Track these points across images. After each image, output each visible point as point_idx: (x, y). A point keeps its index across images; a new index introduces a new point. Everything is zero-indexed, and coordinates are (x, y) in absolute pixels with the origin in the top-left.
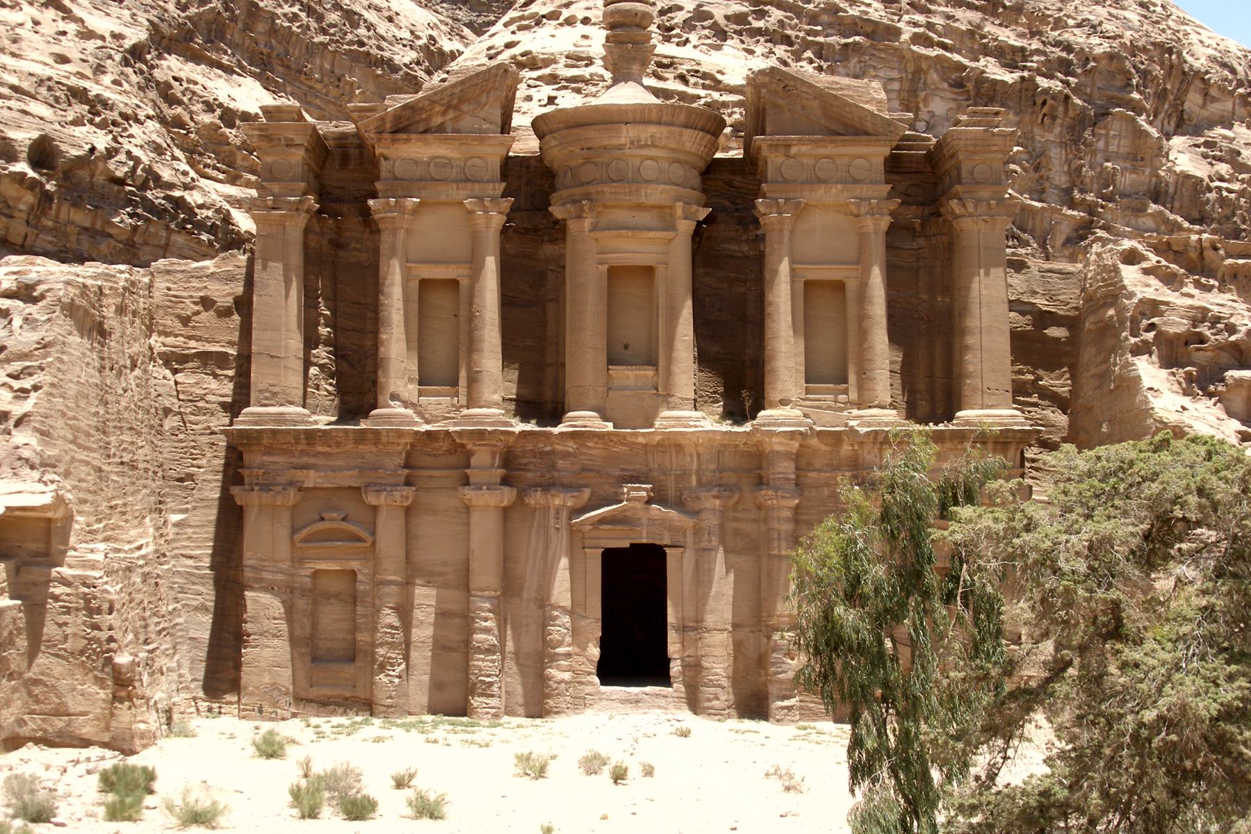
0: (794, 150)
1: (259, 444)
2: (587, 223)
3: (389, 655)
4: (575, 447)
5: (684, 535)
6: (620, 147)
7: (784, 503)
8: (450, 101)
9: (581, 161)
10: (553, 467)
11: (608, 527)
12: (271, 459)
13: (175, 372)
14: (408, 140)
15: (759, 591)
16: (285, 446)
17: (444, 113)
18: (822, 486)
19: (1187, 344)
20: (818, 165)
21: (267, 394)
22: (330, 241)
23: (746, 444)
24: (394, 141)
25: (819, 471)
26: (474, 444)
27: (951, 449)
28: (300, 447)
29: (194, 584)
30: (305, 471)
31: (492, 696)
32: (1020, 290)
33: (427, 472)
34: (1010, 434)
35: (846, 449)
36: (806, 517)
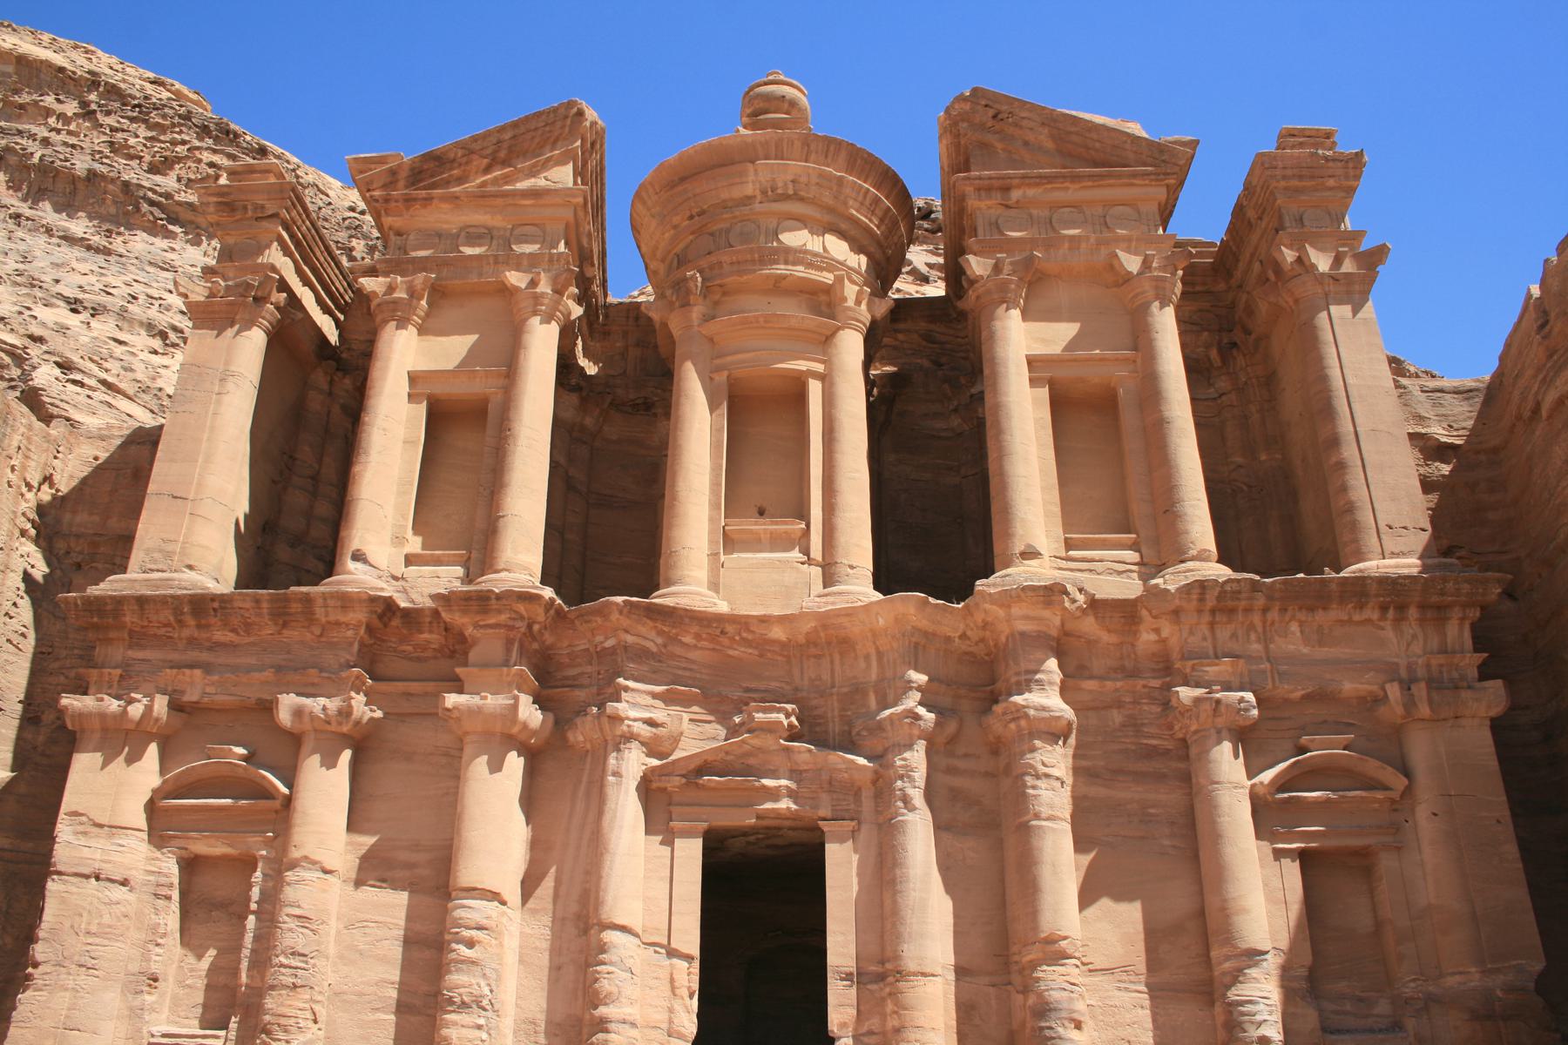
2: (696, 312)
4: (659, 641)
5: (857, 793)
6: (749, 199)
8: (496, 151)
9: (691, 237)
12: (140, 654)
15: (1002, 904)
16: (162, 631)
17: (487, 170)
18: (1108, 707)
21: (156, 555)
22: (344, 408)
23: (963, 636)
25: (1101, 678)
26: (476, 626)
27: (1342, 622)
28: (186, 633)
30: (187, 671)
35: (1146, 638)
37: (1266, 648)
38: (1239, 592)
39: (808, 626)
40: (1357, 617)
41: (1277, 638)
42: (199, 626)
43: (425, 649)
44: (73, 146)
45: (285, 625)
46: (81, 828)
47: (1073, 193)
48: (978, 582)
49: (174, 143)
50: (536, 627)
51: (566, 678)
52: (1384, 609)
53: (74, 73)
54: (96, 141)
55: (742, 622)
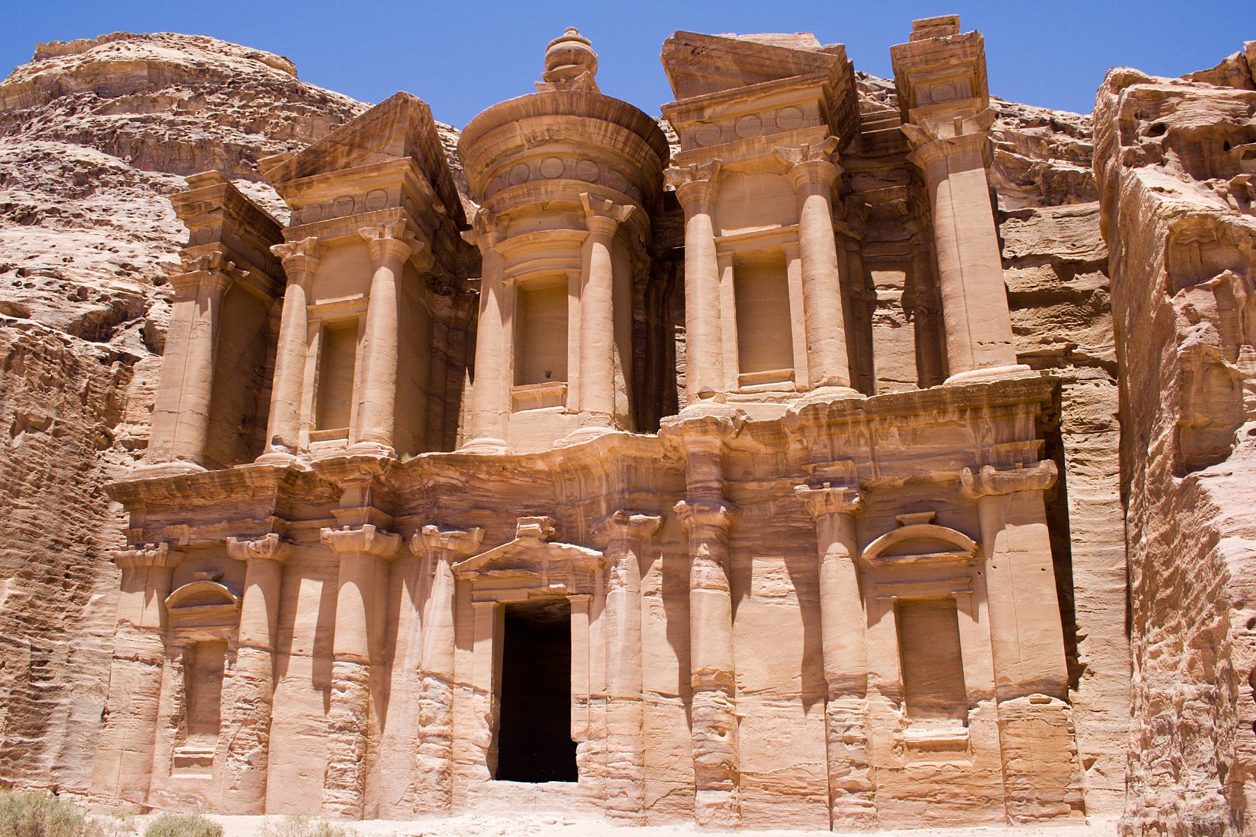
0: (708, 113)
1: (141, 501)
2: (491, 237)
3: (239, 735)
4: (463, 479)
7: (704, 519)
8: (352, 140)
10: (435, 504)
11: (496, 573)
12: (153, 517)
13: (137, 458)
14: (310, 184)
18: (767, 501)
19: (1227, 147)
20: (738, 125)
21: (161, 452)
23: (665, 457)
24: (299, 187)
28: (177, 501)
29: (95, 663)
31: (344, 787)
32: (1031, 244)
33: (307, 524)
34: (1010, 390)
35: (794, 448)
36: (746, 543)
37: (873, 450)
38: (844, 410)
39: (559, 459)
40: (941, 420)
41: (880, 441)
42: (184, 497)
43: (321, 497)
44: (190, 123)
45: (232, 491)
46: (127, 629)
47: (751, 104)
48: (662, 420)
49: (259, 106)
50: (383, 478)
51: (411, 508)
52: (962, 411)
53: (186, 67)
54: (206, 116)
55: (516, 460)
